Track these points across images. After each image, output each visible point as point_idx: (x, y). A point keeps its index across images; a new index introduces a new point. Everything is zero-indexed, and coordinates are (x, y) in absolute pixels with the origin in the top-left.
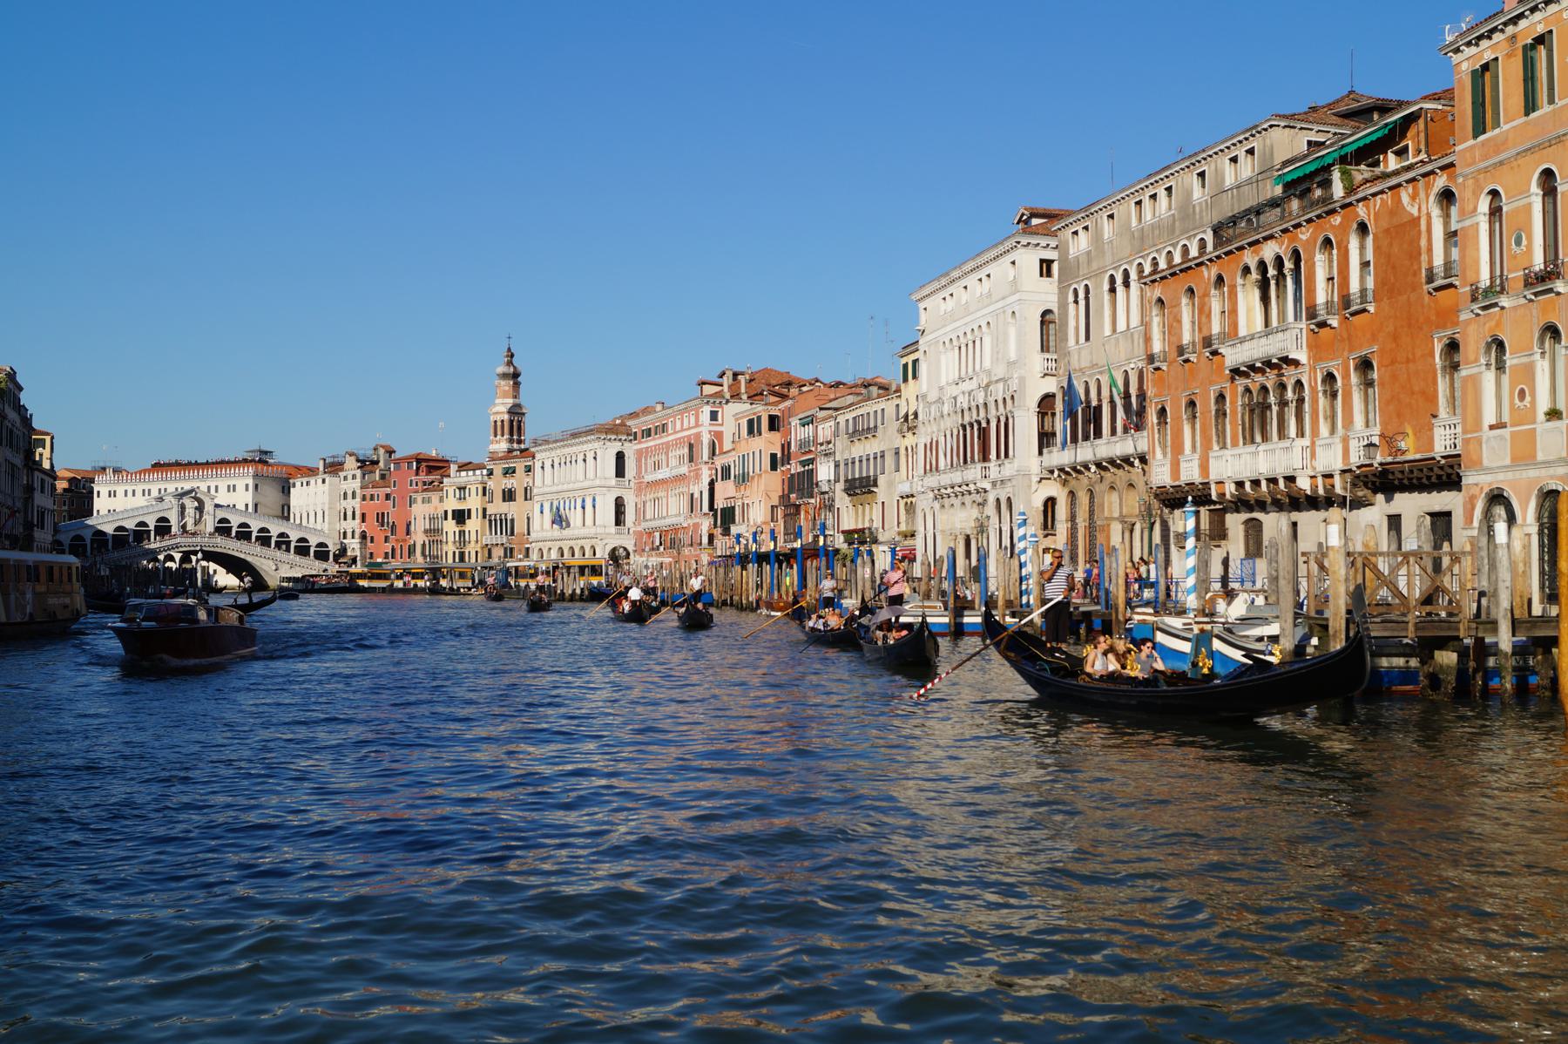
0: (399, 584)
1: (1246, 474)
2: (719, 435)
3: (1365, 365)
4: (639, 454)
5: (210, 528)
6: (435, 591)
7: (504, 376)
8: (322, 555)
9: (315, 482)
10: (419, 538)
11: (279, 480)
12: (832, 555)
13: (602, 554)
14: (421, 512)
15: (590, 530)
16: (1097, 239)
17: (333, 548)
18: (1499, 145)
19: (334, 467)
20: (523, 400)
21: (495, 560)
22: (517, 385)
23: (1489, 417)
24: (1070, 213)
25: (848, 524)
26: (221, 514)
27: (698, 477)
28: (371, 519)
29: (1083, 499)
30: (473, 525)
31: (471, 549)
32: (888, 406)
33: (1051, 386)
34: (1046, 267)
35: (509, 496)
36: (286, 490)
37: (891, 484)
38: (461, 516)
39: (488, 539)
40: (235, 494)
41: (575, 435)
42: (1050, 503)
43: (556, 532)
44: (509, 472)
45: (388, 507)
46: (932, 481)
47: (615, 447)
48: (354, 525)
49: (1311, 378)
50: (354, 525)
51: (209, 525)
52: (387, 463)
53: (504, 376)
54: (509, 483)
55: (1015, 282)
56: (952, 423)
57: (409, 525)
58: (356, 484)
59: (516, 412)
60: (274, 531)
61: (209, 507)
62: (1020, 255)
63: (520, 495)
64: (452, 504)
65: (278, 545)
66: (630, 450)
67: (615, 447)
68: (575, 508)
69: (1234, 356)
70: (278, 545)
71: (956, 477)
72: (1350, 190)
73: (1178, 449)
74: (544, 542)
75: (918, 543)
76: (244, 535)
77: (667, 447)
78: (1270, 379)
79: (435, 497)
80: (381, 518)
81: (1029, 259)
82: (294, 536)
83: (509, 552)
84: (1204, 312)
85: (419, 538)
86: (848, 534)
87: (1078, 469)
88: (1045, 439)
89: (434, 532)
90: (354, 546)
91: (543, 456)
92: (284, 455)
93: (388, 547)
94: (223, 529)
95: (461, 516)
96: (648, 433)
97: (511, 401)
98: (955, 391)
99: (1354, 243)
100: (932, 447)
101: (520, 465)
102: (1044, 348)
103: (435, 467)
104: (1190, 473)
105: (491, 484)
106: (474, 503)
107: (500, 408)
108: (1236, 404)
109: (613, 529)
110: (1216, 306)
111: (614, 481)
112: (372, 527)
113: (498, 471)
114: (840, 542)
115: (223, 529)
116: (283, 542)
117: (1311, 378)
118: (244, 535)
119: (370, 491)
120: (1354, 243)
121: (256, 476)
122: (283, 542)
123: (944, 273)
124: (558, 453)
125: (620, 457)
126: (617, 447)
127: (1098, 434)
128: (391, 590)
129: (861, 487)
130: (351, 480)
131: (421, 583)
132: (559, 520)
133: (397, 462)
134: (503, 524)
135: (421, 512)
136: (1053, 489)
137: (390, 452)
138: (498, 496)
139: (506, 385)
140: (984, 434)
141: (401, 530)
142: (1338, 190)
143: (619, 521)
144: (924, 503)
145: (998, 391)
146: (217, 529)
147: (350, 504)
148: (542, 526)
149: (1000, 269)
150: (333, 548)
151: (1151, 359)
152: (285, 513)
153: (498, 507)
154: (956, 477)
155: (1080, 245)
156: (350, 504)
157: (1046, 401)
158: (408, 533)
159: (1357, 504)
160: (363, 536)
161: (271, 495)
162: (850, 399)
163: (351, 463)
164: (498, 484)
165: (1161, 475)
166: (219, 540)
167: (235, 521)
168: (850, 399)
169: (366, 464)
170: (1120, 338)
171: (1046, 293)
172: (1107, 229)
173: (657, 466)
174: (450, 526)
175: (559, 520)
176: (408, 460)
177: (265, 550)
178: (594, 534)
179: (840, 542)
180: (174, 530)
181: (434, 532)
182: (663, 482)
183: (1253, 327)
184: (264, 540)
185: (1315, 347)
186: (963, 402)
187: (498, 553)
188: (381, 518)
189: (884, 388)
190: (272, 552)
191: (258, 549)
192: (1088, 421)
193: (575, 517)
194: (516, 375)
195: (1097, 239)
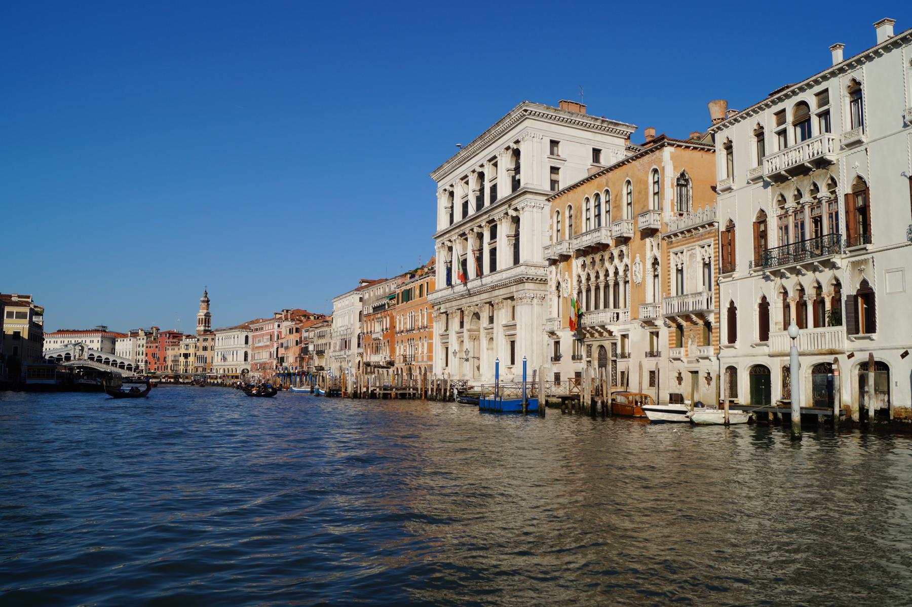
0: (164, 380)
2: (280, 332)
5: (86, 358)
6: (177, 383)
10: (169, 363)
11: (111, 339)
13: (239, 372)
14: (170, 353)
17: (133, 366)
19: (135, 334)
20: (210, 311)
21: (199, 372)
26: (91, 352)
27: (273, 346)
28: (150, 355)
30: (191, 359)
31: (190, 368)
35: (205, 349)
36: (114, 343)
38: (186, 356)
39: (196, 365)
40: (94, 343)
43: (223, 363)
46: (334, 354)
47: (245, 334)
48: (143, 357)
50: (143, 357)
51: (86, 356)
52: (157, 334)
54: (205, 344)
57: (165, 358)
58: (144, 342)
59: (207, 315)
60: (111, 359)
61: (86, 349)
63: (209, 349)
64: (183, 351)
65: (112, 365)
66: (250, 335)
67: (245, 334)
68: (230, 354)
70: (112, 365)
74: (219, 366)
76: (99, 360)
77: (263, 335)
79: (176, 348)
80: (154, 355)
82: (119, 361)
83: (204, 369)
85: (169, 363)
89: (175, 361)
90: (142, 365)
91: (219, 335)
92: (112, 328)
93: (156, 366)
94: (91, 358)
95: (186, 356)
96: (257, 330)
101: (210, 338)
103: (176, 337)
106: (191, 351)
107: (201, 314)
112: (150, 358)
113: (201, 339)
115: (91, 358)
118: (99, 360)
119: (149, 345)
121: (102, 337)
124: (224, 335)
125: (247, 337)
126: (246, 334)
128: (161, 382)
129: (320, 353)
133: (161, 334)
134: (203, 359)
135: (170, 353)
137: (158, 330)
138: (201, 349)
141: (161, 360)
143: (246, 359)
147: (141, 349)
148: (217, 361)
150: (133, 366)
152: (113, 351)
153: (201, 353)
156: (141, 349)
158: (165, 361)
160: (146, 362)
161: (108, 344)
164: (201, 344)
167: (96, 355)
169: (148, 334)
173: (259, 341)
174: (182, 359)
175: (224, 359)
176: (165, 333)
178: (236, 363)
180: (72, 358)
181: (175, 361)
187: (200, 370)
188: (154, 355)
193: (229, 358)
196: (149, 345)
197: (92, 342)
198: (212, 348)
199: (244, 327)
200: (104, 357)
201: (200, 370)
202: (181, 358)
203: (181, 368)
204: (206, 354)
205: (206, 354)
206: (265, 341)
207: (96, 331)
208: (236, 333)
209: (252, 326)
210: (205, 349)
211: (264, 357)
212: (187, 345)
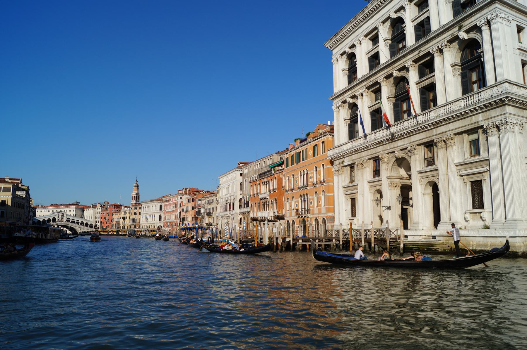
0: (110, 233)
1: (261, 216)
2: (182, 202)
3: (276, 200)
4: (165, 206)
5: (65, 220)
6: (118, 235)
7: (135, 186)
8: (91, 226)
9: (90, 210)
10: (114, 223)
11: (81, 209)
12: (202, 228)
13: (156, 227)
14: (115, 217)
15: (153, 222)
16: (249, 170)
17: (94, 225)
18: (288, 170)
19: (95, 206)
20: (139, 192)
21: (132, 228)
22: (138, 188)
23: (288, 209)
24: (248, 163)
25: (207, 222)
26: (68, 217)
27: (177, 211)
28: (103, 218)
29: (246, 218)
30: (127, 220)
31: (126, 226)
32: (214, 198)
33: (241, 197)
34: (241, 175)
35: (135, 214)
36: (83, 211)
37: (215, 214)
38: (124, 218)
39: (130, 224)
40: (71, 212)
41: (151, 201)
42: (241, 218)
43: (146, 222)
44: (136, 208)
45: (107, 216)
47: (160, 204)
48: (99, 220)
49: (270, 201)
50: (99, 220)
51: (65, 219)
53: (135, 186)
55: (235, 177)
56: (225, 203)
59: (138, 194)
60: (80, 221)
61: (65, 215)
62: (236, 172)
64: (122, 215)
65: (81, 224)
66: (163, 204)
67: (160, 204)
68: (150, 217)
69: (261, 196)
70: (81, 224)
71: (225, 213)
72: (275, 172)
73: (253, 211)
75: (219, 226)
76: (73, 222)
77: (171, 204)
78: (265, 201)
79: (118, 214)
80: (105, 218)
81: (238, 173)
82: (85, 222)
83: (135, 226)
84: (257, 189)
85: (114, 223)
86: (207, 224)
87: (245, 213)
88: (240, 207)
89: (118, 222)
90: (99, 224)
91: (143, 205)
92: (82, 203)
94: (68, 220)
95: (124, 218)
96: (167, 201)
97: (136, 192)
98: (225, 197)
99: (275, 181)
100: (221, 207)
101: (138, 207)
102: (241, 190)
103: (118, 207)
104: (255, 216)
105: (131, 211)
106: (127, 215)
107: (134, 194)
108: (261, 204)
109: (159, 222)
110: (259, 188)
111: (159, 211)
112: (103, 220)
113: (133, 208)
114: (205, 226)
115: (68, 220)
116: (82, 224)
117: (270, 201)
118: (73, 222)
119: (103, 212)
120: (275, 181)
122: (82, 224)
123: (224, 174)
125: (161, 206)
127: (248, 206)
128: (108, 235)
129: (209, 214)
130: (99, 209)
131: (115, 233)
132: (147, 219)
133: (110, 206)
134: (134, 220)
135: (115, 217)
136: (241, 216)
137: (108, 203)
138: (133, 214)
139: (136, 188)
140: (230, 205)
142: (273, 172)
143: (160, 220)
144: (220, 218)
145: (232, 197)
146: (67, 221)
148: (143, 221)
149: (233, 174)
150: (94, 225)
151: (250, 195)
152: (82, 217)
153: (133, 216)
154: (225, 213)
155: (246, 171)
156: (98, 215)
157: (240, 199)
159: (275, 221)
160: (101, 222)
161: (79, 212)
162: (208, 196)
163: (99, 206)
164: (133, 211)
165: (251, 216)
166: (67, 223)
167: (71, 218)
168: (208, 196)
169: (102, 206)
170: (249, 191)
171: (240, 179)
172: (250, 169)
173: (169, 208)
174: (122, 220)
175: (147, 219)
176: (112, 205)
177: (78, 225)
178: (154, 222)
179: (205, 226)
180: (57, 220)
181: (118, 222)
182: (170, 212)
183: (264, 191)
184: (78, 223)
185: (270, 196)
186: (226, 199)
187: (133, 227)
188: (105, 218)
189: (214, 194)
190: (80, 226)
191: (76, 225)
192: (247, 204)
193: (150, 219)
194: (138, 186)
195: (249, 170)
196: (103, 212)
197: (70, 211)
198: (140, 214)
199: (159, 200)
200: (76, 220)
201: (133, 227)
202: (121, 220)
203: (121, 226)
204: (136, 217)
205: (136, 217)
206: (172, 208)
207: (73, 204)
208: (154, 203)
209: (164, 199)
210: (135, 214)
211: (171, 218)
212: (125, 212)
